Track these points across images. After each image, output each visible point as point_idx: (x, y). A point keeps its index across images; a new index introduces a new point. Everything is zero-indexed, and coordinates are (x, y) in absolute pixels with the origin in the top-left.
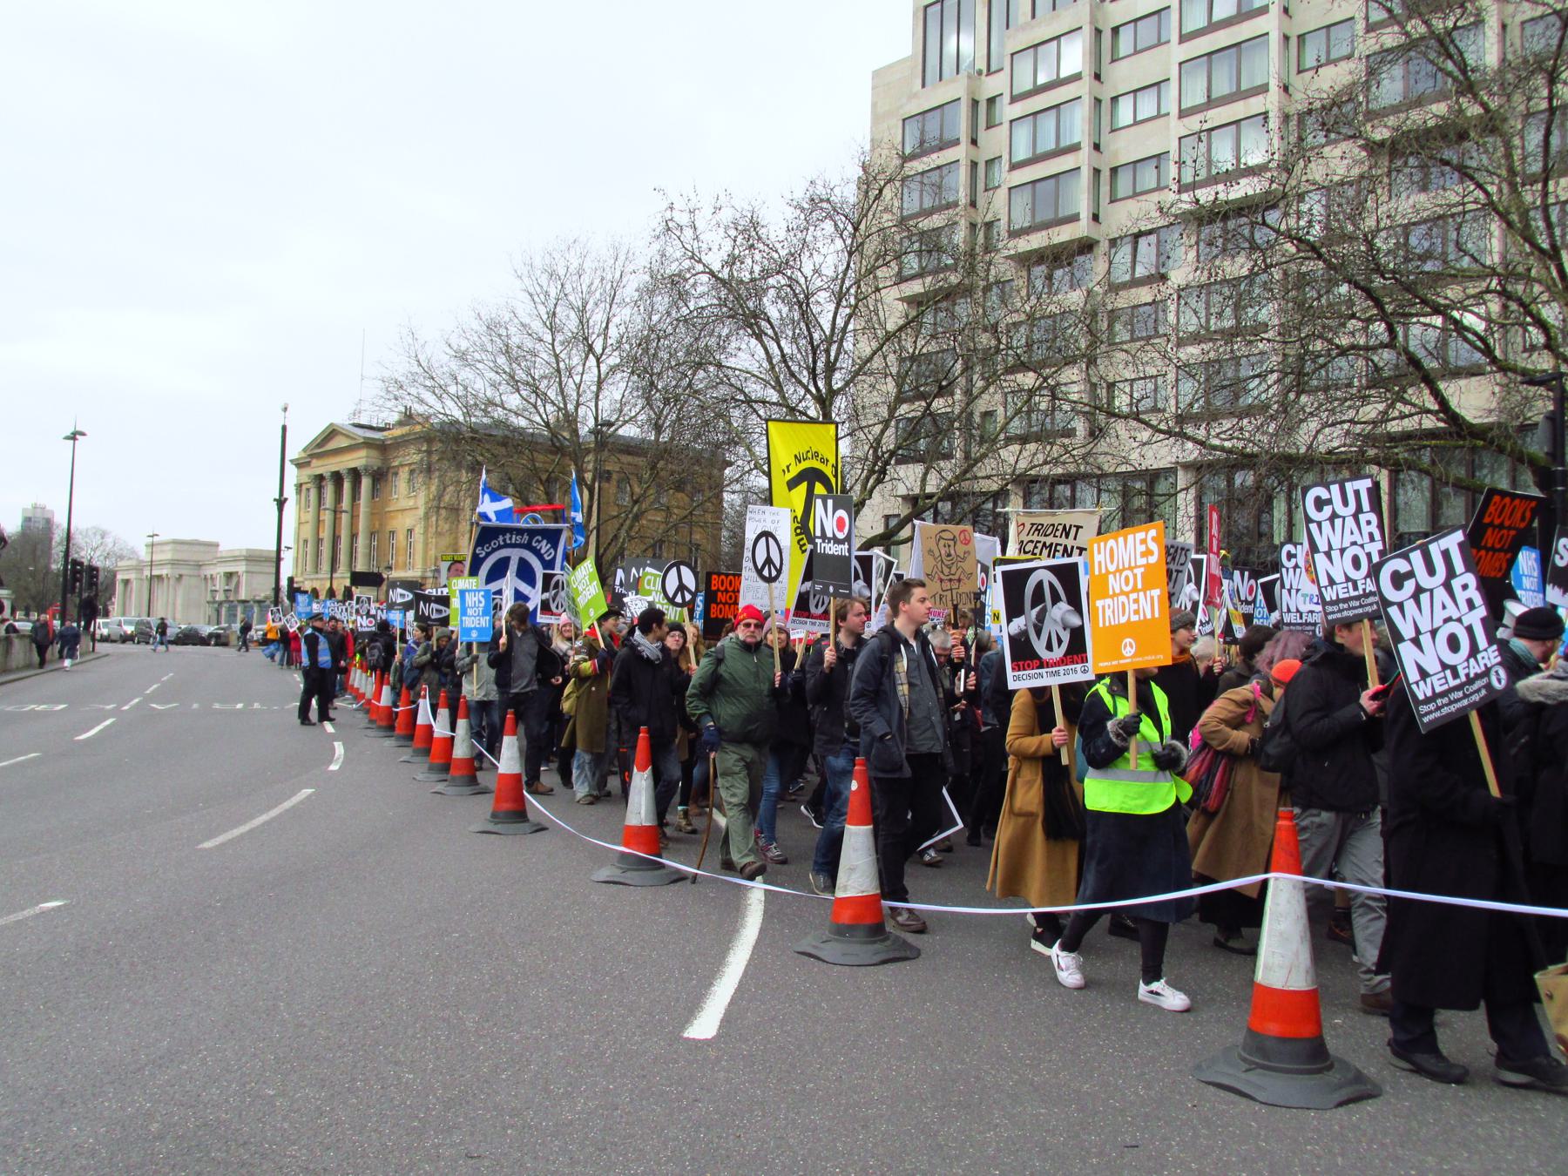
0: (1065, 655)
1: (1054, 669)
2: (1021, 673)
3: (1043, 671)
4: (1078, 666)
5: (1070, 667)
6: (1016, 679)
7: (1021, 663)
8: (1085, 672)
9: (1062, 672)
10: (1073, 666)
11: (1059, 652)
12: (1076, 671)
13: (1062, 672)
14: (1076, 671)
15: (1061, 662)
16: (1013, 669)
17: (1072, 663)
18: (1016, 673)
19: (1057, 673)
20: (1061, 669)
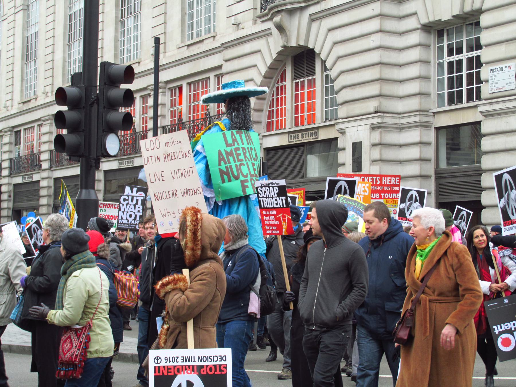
0: (175, 376)
1: (188, 363)
2: (218, 363)
3: (198, 363)
4: (163, 364)
5: (172, 364)
6: (222, 358)
7: (218, 372)
8: (158, 358)
9: (180, 360)
10: (168, 364)
11: (181, 379)
12: (166, 359)
13: (180, 360)
14: (166, 359)
15: (179, 370)
16: (225, 367)
17: (169, 368)
18: (222, 363)
19: (185, 359)
20: (180, 363)
